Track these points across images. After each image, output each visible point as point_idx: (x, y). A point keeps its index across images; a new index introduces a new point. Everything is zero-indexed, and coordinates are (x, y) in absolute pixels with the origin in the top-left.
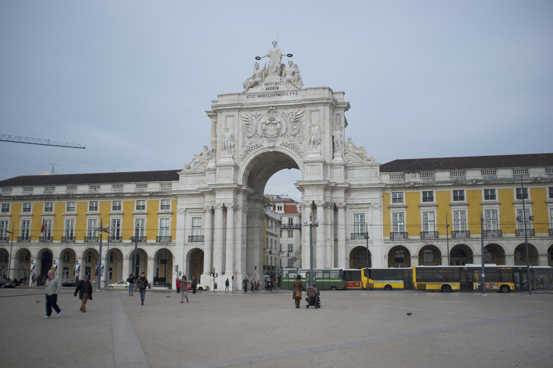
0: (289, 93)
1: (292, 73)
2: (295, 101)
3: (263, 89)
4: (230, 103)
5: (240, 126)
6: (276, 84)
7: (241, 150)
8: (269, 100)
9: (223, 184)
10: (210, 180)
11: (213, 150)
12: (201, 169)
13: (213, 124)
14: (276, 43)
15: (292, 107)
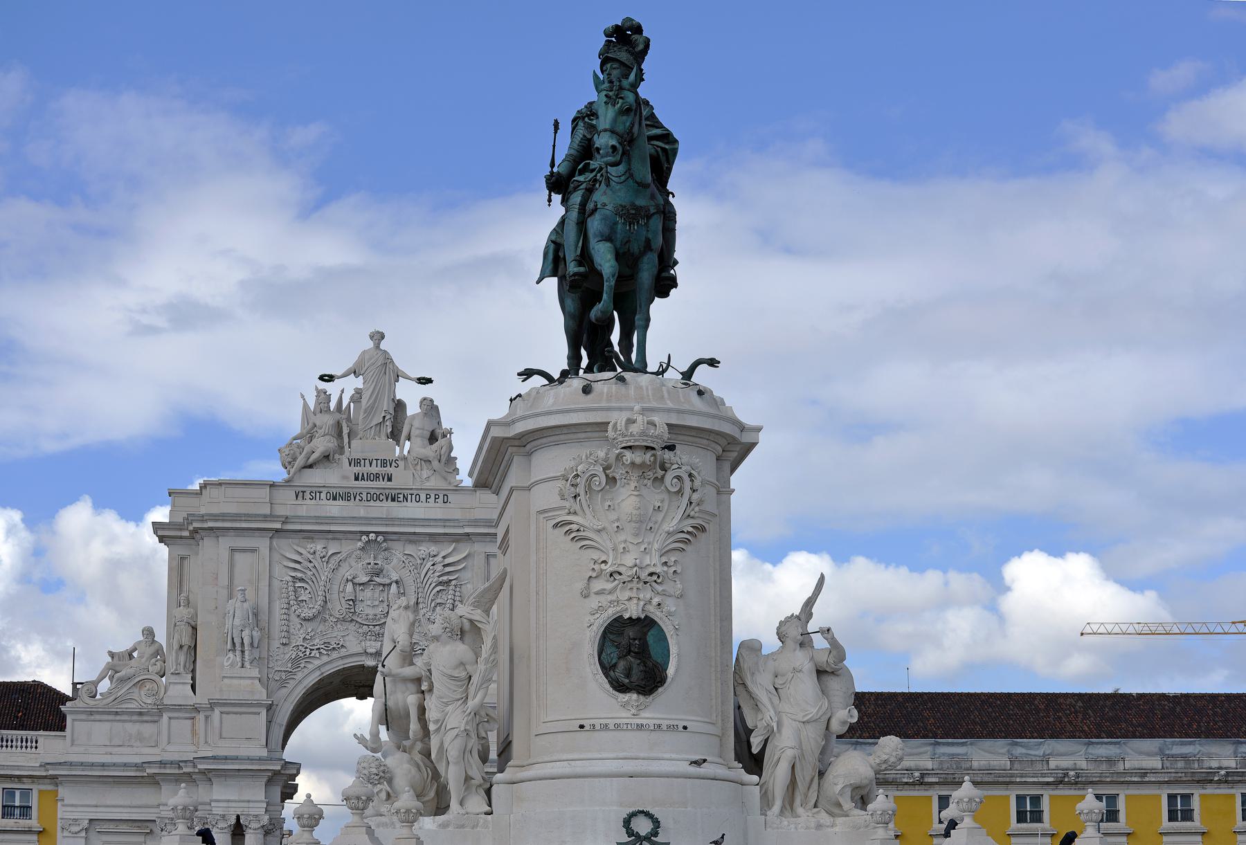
0: (423, 497)
1: (428, 435)
2: (445, 522)
3: (345, 477)
4: (243, 510)
5: (276, 583)
6: (384, 463)
7: (282, 658)
8: (362, 512)
9: (236, 759)
10: (177, 742)
11: (181, 647)
12: (142, 699)
13: (175, 563)
14: (382, 336)
15: (433, 538)
